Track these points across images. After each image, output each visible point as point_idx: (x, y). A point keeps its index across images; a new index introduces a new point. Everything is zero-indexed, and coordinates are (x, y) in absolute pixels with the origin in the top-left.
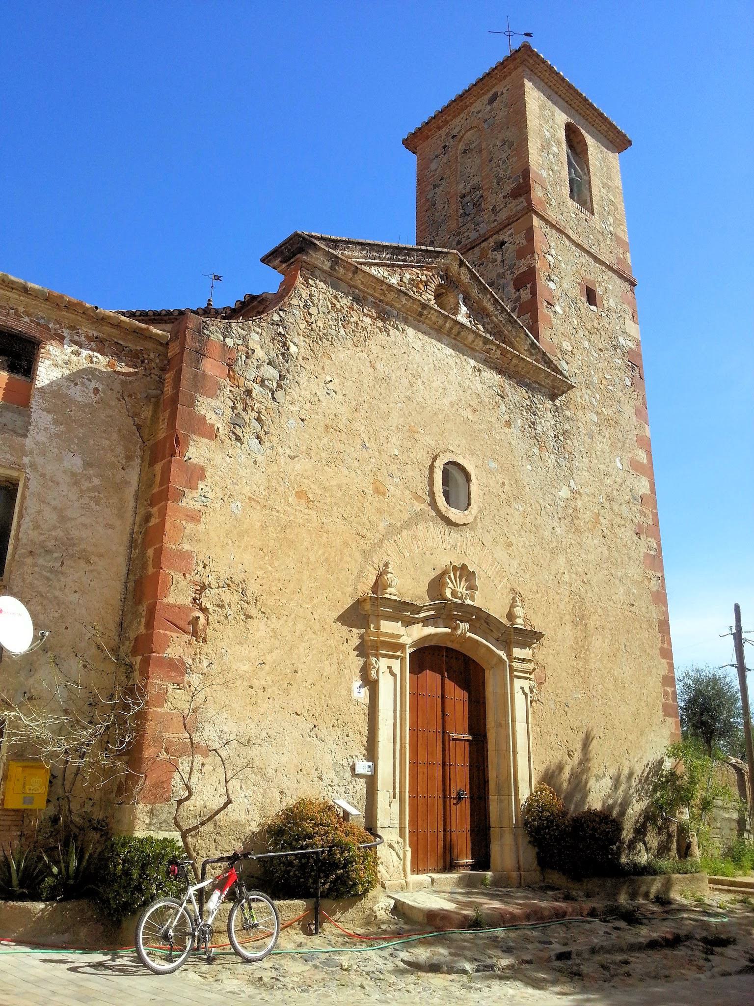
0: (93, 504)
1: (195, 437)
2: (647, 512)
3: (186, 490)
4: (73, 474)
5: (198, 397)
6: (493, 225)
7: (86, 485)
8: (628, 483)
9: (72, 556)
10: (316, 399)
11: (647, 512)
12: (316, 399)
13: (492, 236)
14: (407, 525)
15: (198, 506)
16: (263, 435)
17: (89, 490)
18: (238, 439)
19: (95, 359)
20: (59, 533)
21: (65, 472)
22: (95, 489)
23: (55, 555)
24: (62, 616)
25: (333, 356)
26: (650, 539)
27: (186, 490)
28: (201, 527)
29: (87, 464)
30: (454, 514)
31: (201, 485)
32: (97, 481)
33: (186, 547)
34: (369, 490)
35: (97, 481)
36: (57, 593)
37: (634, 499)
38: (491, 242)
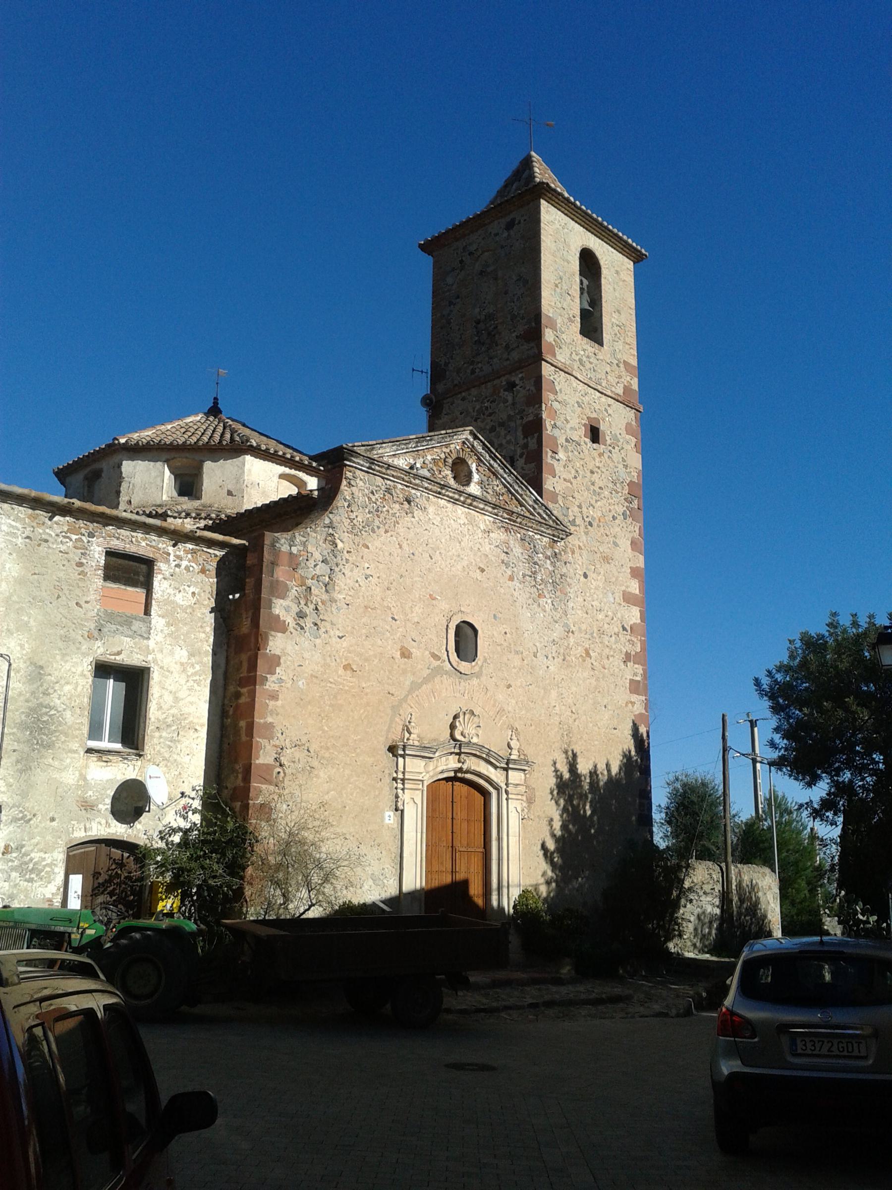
0: (195, 685)
1: (273, 633)
2: (635, 640)
3: (268, 676)
4: (182, 664)
5: (274, 601)
6: (505, 363)
7: (191, 671)
8: (619, 615)
9: (184, 727)
10: (357, 585)
11: (635, 640)
12: (357, 585)
13: (504, 375)
14: (426, 680)
15: (276, 687)
16: (319, 622)
17: (192, 675)
18: (302, 628)
19: (191, 569)
20: (174, 711)
21: (176, 663)
22: (195, 674)
23: (173, 728)
24: (180, 774)
25: (370, 545)
26: (636, 666)
27: (268, 676)
28: (279, 703)
29: (191, 655)
30: (464, 666)
31: (278, 670)
32: (198, 667)
33: (269, 720)
34: (398, 655)
35: (198, 667)
36: (175, 756)
37: (624, 629)
38: (503, 381)
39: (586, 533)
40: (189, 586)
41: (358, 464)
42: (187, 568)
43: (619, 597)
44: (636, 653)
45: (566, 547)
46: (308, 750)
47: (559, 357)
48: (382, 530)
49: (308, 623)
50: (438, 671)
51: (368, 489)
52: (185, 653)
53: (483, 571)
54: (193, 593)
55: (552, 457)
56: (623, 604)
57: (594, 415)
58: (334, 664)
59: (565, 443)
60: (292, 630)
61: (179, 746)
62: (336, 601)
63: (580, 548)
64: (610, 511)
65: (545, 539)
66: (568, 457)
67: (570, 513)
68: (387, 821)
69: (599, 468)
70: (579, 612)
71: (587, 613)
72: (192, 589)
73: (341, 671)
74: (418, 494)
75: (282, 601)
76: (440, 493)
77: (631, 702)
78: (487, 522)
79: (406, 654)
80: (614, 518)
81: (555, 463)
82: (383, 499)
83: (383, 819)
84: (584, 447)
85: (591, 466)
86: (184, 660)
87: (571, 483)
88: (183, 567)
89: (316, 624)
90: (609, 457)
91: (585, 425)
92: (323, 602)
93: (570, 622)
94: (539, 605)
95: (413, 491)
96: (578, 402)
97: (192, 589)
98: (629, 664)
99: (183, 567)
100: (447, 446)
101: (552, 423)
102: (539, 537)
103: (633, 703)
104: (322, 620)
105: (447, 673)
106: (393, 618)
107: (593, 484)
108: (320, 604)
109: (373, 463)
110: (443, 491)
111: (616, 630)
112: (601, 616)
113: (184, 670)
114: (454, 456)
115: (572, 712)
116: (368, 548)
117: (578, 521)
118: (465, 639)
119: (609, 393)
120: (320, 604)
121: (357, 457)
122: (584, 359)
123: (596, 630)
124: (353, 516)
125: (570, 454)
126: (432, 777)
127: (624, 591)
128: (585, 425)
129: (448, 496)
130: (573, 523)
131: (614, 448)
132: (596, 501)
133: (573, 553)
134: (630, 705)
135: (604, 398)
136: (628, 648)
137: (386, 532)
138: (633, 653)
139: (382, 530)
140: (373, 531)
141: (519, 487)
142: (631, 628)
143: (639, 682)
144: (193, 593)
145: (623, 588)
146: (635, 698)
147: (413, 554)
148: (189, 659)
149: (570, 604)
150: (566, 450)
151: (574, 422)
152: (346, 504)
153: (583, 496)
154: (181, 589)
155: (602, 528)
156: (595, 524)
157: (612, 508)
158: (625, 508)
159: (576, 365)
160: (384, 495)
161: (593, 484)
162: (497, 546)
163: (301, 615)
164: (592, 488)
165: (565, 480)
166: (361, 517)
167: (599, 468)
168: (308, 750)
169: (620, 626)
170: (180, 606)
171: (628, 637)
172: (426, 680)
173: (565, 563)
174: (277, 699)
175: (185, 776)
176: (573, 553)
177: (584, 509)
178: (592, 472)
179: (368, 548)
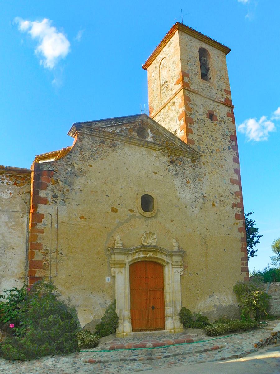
0: (13, 230)
1: (39, 205)
2: (237, 198)
3: (37, 223)
4: (6, 222)
5: (39, 191)
6: (171, 96)
7: (10, 225)
8: (229, 188)
9: (8, 248)
10: (86, 182)
11: (237, 198)
12: (86, 182)
13: (171, 100)
14: (127, 221)
15: (42, 228)
16: (65, 199)
17: (11, 226)
18: (56, 202)
19: (9, 183)
20: (3, 241)
21: (3, 222)
22: (13, 226)
23: (2, 248)
24: (6, 267)
25: (92, 165)
26: (238, 208)
27: (37, 223)
28: (45, 234)
29: (10, 218)
30: (147, 214)
31: (43, 220)
32: (13, 223)
33: (39, 242)
34: (110, 211)
35: (13, 223)
36: (4, 260)
37: (231, 194)
38: (171, 103)
39: (210, 156)
40: (8, 190)
41: (84, 131)
42: (7, 183)
43: (228, 181)
44: (238, 203)
45: (200, 162)
46: (61, 254)
47: (191, 87)
48: (99, 159)
49: (59, 199)
50: (134, 217)
51: (91, 142)
52: (7, 218)
53: (156, 173)
54: (11, 193)
55: (190, 126)
56: (230, 184)
57: (211, 109)
58: (74, 216)
59: (197, 121)
60: (50, 203)
61: (6, 256)
62: (74, 190)
63: (207, 162)
64: (222, 147)
65: (189, 159)
66: (199, 126)
67: (201, 148)
68: (107, 281)
69: (215, 130)
70: (209, 188)
71: (212, 188)
72: (10, 191)
73: (78, 219)
74: (119, 143)
75: (44, 191)
76: (130, 142)
77: (236, 223)
78: (157, 153)
79: (114, 210)
80: (224, 149)
81: (192, 129)
82: (100, 146)
83: (105, 280)
84: (207, 122)
85: (211, 129)
86: (7, 221)
87: (201, 136)
88: (5, 183)
89: (63, 200)
90: (220, 126)
91: (207, 113)
92: (68, 191)
93: (204, 192)
94: (187, 186)
95: (116, 142)
96: (202, 105)
97: (10, 191)
98: (234, 208)
99: (5, 183)
100: (134, 123)
101: (190, 113)
102: (185, 158)
103: (237, 224)
104: (67, 198)
105: (138, 217)
106: (107, 196)
107: (212, 136)
108: (65, 191)
109: (92, 131)
110: (132, 141)
111: (227, 194)
112: (219, 189)
113: (7, 225)
114: (138, 126)
115: (206, 229)
116: (92, 166)
117: (206, 151)
118: (147, 203)
119: (217, 101)
120: (65, 191)
121: (82, 128)
122: (204, 88)
123: (217, 195)
124: (83, 153)
125: (200, 125)
126: (131, 261)
127: (231, 179)
128: (207, 113)
129: (134, 143)
130: (203, 152)
131: (222, 122)
132: (215, 143)
133: (204, 164)
134: (236, 224)
135: (215, 103)
136: (234, 201)
137: (102, 159)
138: (236, 203)
139: (99, 159)
140: (94, 159)
141: (173, 137)
142: (235, 193)
143: (240, 214)
144: (11, 193)
145: (230, 177)
146: (238, 221)
147: (117, 168)
148: (9, 220)
149: (204, 185)
150: (197, 123)
151: (201, 111)
152: (79, 149)
153: (208, 141)
154: (4, 191)
155: (218, 154)
156: (215, 152)
157: (222, 145)
158: (229, 146)
159: (200, 90)
160: (100, 144)
161: (212, 136)
162: (164, 163)
163: (55, 196)
164: (212, 138)
165: (198, 135)
166: (87, 153)
167: (215, 130)
168: (61, 254)
169: (229, 193)
170: (4, 199)
171: (234, 197)
172: (127, 221)
173: (200, 168)
174: (43, 233)
175: (9, 268)
176: (204, 164)
177: (208, 146)
178: (212, 132)
179: (92, 166)
